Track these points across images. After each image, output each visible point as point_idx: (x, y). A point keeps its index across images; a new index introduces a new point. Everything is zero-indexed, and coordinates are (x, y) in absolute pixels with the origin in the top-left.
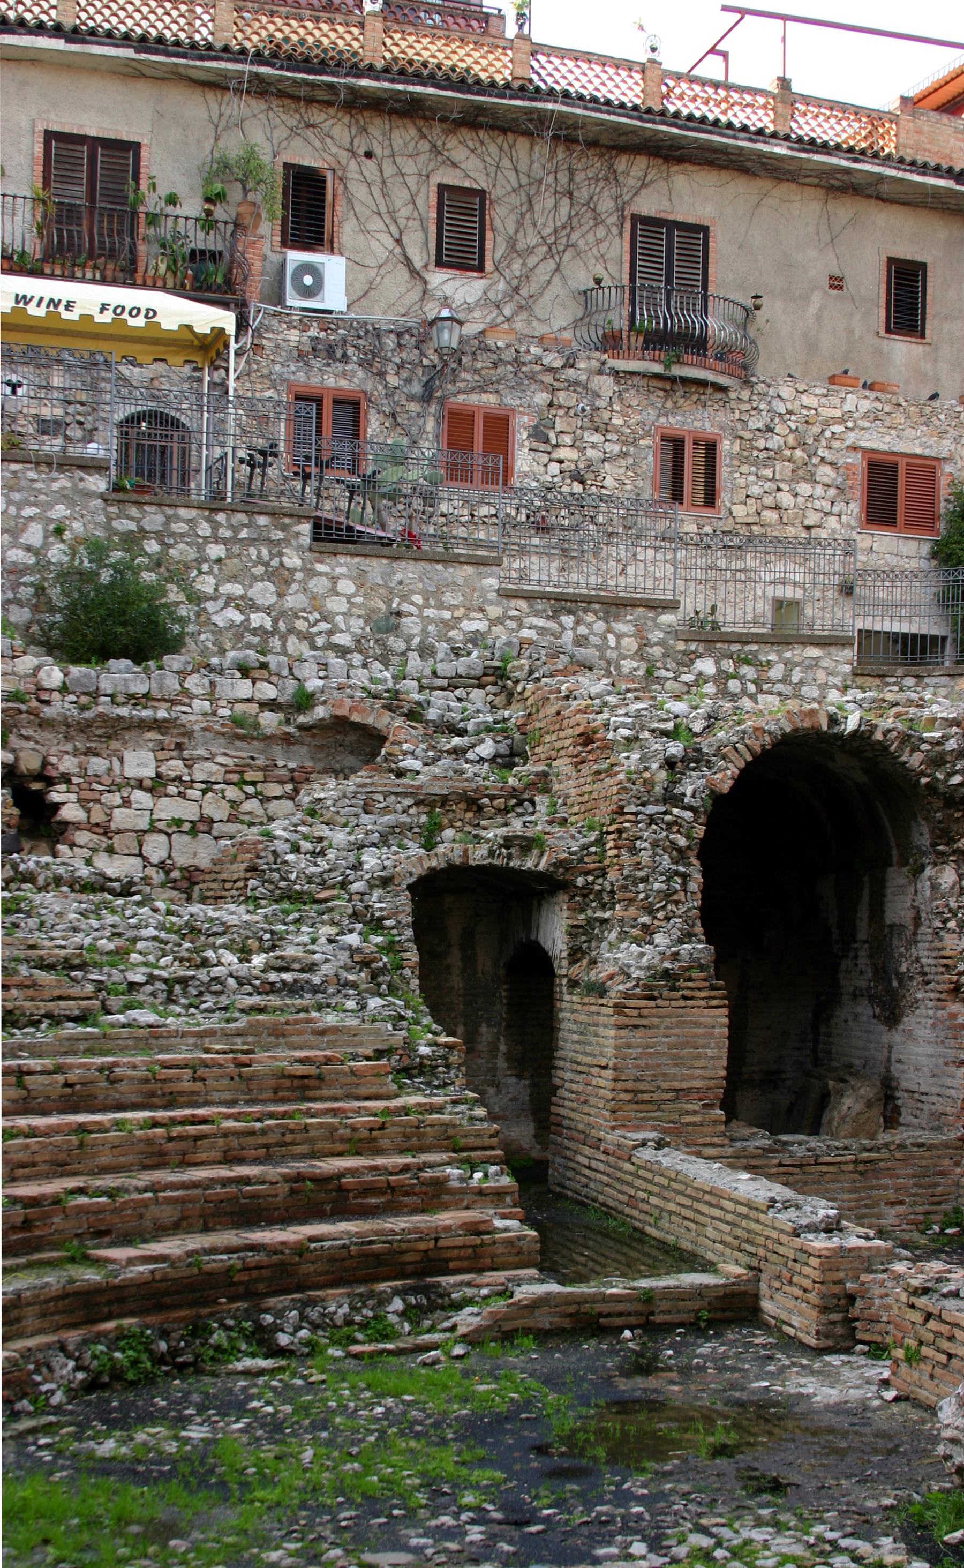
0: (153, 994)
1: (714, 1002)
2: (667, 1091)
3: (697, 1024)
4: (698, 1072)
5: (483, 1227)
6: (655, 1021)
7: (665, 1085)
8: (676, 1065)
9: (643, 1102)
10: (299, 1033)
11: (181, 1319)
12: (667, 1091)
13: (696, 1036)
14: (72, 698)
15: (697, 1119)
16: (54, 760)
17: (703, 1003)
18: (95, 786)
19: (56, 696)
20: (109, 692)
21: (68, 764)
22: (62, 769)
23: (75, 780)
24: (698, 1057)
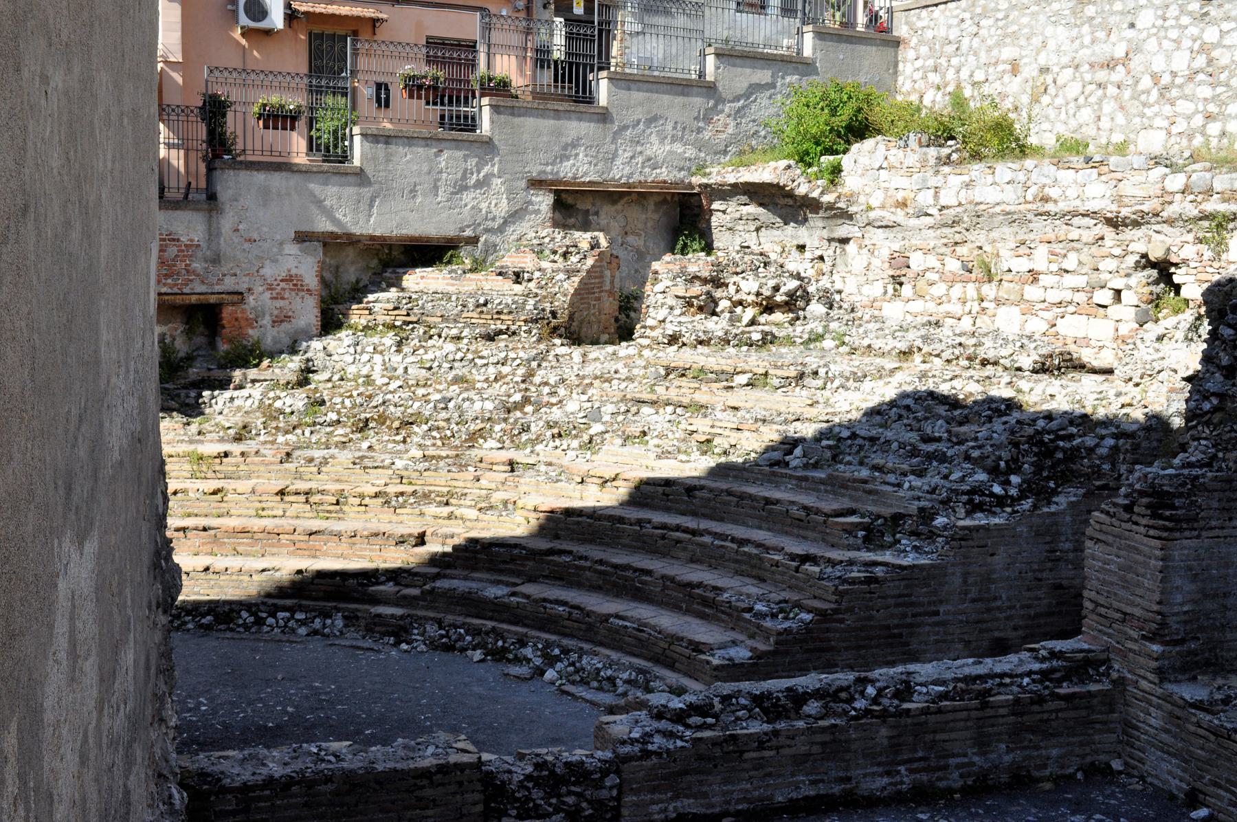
0: (850, 446)
1: (1152, 532)
2: (1118, 611)
3: (1139, 552)
4: (1138, 600)
5: (701, 647)
6: (1110, 539)
7: (1116, 604)
8: (1123, 587)
9: (1101, 615)
10: (856, 489)
11: (516, 633)
12: (1118, 611)
13: (1136, 562)
14: (1192, 197)
15: (1135, 647)
16: (1174, 249)
17: (1142, 529)
18: (1208, 269)
19: (1178, 197)
20: (1219, 190)
21: (1189, 252)
22: (1182, 256)
23: (1192, 264)
24: (1138, 585)
